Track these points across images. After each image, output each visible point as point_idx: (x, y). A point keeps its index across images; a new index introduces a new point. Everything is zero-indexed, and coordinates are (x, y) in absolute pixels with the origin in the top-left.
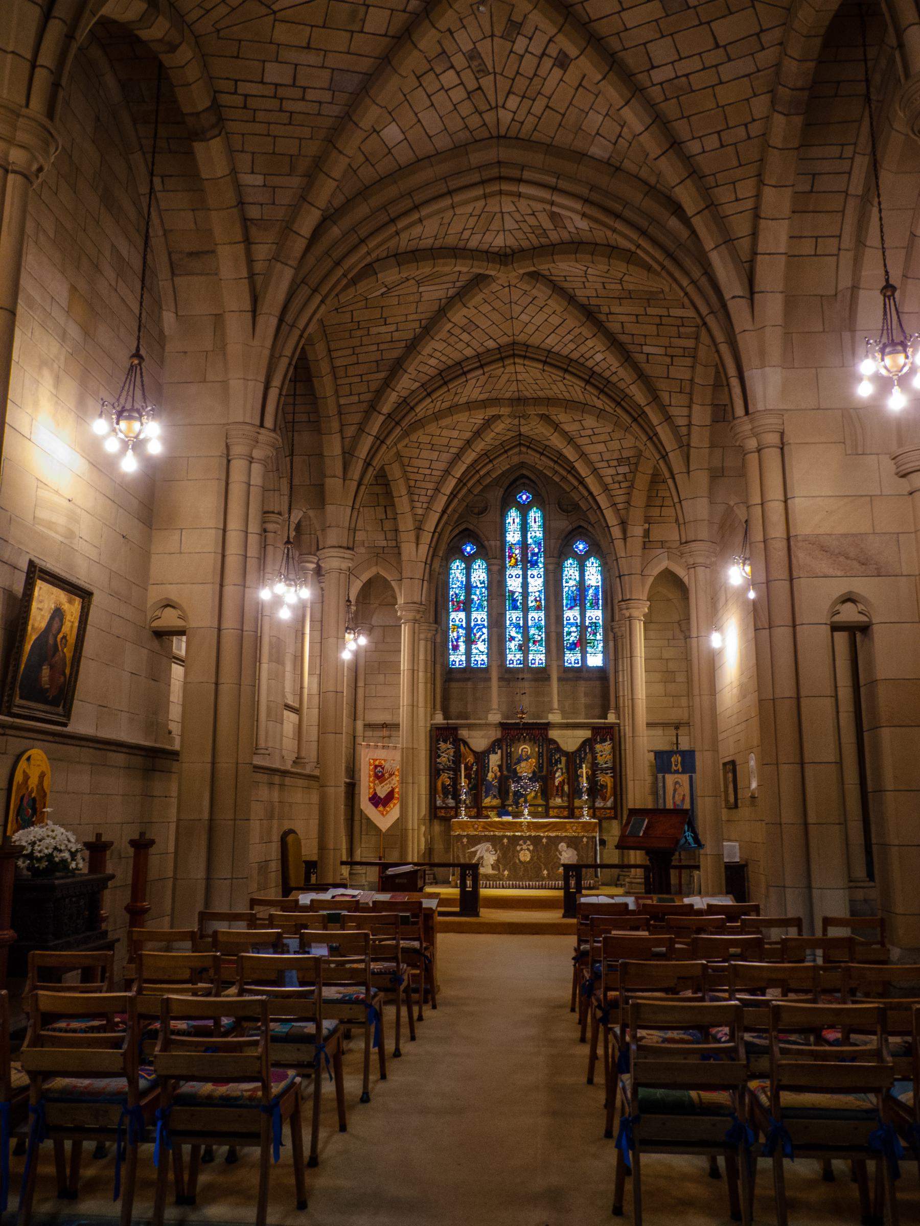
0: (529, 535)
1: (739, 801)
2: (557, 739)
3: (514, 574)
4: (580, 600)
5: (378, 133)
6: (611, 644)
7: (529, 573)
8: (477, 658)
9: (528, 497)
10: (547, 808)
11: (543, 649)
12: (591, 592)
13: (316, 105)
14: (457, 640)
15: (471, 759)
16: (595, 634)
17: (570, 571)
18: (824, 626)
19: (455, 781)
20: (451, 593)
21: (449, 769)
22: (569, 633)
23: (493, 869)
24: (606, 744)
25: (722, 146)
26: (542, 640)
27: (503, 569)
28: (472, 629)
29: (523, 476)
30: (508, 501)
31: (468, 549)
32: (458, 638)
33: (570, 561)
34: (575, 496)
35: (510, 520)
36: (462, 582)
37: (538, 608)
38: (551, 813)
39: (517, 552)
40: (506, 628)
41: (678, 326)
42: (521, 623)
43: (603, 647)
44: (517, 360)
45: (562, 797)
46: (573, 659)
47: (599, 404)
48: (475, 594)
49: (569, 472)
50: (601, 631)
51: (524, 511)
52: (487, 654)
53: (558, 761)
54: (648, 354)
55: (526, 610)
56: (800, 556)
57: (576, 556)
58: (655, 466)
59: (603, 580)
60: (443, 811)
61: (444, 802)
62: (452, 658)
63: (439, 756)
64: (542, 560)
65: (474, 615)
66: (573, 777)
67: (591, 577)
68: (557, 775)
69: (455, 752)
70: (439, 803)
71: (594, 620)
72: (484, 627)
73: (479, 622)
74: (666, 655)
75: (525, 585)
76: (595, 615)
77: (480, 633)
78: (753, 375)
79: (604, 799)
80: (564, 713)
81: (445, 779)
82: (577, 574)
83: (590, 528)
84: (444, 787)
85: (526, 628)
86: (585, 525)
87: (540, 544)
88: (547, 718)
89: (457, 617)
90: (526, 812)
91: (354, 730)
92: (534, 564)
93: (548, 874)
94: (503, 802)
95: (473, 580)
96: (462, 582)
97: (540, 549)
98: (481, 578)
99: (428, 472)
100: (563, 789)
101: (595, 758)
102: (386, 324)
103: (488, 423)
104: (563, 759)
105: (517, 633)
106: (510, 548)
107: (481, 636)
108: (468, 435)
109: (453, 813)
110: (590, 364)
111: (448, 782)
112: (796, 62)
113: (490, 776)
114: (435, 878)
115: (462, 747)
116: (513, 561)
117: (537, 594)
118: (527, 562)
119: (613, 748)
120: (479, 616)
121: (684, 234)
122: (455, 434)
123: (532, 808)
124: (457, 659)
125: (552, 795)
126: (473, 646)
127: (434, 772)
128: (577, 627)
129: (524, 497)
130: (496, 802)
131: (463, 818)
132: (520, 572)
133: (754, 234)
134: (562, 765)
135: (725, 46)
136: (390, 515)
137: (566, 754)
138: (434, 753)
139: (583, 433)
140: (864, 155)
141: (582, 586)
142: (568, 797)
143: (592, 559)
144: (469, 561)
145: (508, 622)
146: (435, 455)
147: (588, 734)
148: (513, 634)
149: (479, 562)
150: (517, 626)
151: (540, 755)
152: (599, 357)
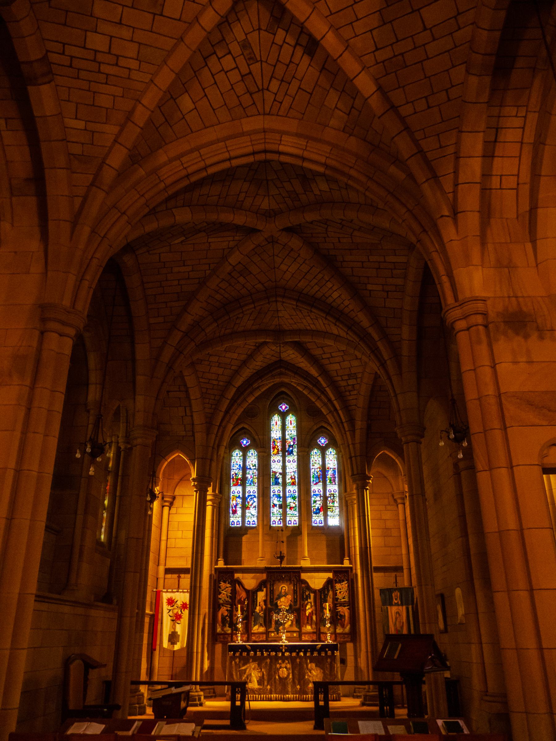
0: (287, 433)
1: (449, 627)
2: (308, 581)
3: (276, 460)
5: (175, 100)
6: (344, 508)
7: (287, 459)
8: (249, 520)
9: (286, 407)
10: (300, 633)
11: (296, 513)
12: (330, 473)
13: (127, 71)
14: (236, 507)
15: (243, 595)
16: (333, 502)
17: (315, 458)
18: (536, 467)
19: (231, 613)
20: (232, 473)
21: (227, 603)
22: (315, 502)
23: (258, 685)
24: (344, 583)
25: (429, 107)
26: (296, 505)
27: (269, 455)
28: (247, 499)
29: (283, 393)
30: (274, 409)
31: (245, 442)
32: (237, 505)
33: (315, 450)
34: (318, 404)
35: (273, 423)
36: (240, 465)
37: (293, 484)
38: (303, 638)
39: (279, 444)
40: (270, 498)
41: (392, 269)
42: (281, 494)
43: (340, 511)
44: (279, 299)
45: (311, 625)
46: (318, 521)
47: (335, 332)
48: (249, 474)
49: (314, 385)
50: (337, 499)
51: (284, 416)
52: (257, 517)
53: (308, 597)
54: (370, 290)
55: (284, 485)
56: (511, 409)
58: (377, 377)
59: (338, 464)
60: (222, 637)
61: (222, 629)
62: (232, 519)
63: (220, 593)
65: (248, 488)
66: (320, 610)
67: (330, 462)
68: (307, 608)
69: (232, 590)
70: (219, 630)
71: (332, 493)
72: (255, 497)
73: (251, 494)
74: (384, 517)
75: (284, 467)
76: (333, 488)
77: (252, 502)
78: (460, 273)
79: (343, 626)
80: (313, 561)
81: (223, 611)
82: (320, 460)
83: (329, 428)
84: (224, 618)
85: (285, 498)
86: (326, 426)
87: (295, 438)
88: (300, 564)
89: (236, 490)
90: (284, 637)
91: (157, 573)
92: (291, 453)
93: (300, 689)
94: (266, 630)
95: (247, 465)
96: (240, 465)
97: (294, 443)
98: (254, 463)
99: (215, 383)
100: (312, 619)
101: (336, 594)
102: (184, 266)
103: (259, 347)
104: (312, 595)
106: (274, 442)
108: (243, 357)
109: (229, 639)
110: (330, 300)
111: (226, 613)
112: (486, 32)
113: (258, 609)
114: (214, 692)
115: (237, 585)
116: (276, 451)
117: (293, 474)
118: (285, 452)
119: (348, 586)
120: (252, 489)
121: (402, 176)
122: (235, 356)
123: (289, 634)
124: (235, 520)
125: (304, 624)
126: (247, 511)
127: (215, 605)
128: (320, 497)
129: (284, 407)
130: (262, 629)
132: (281, 459)
133: (456, 172)
134: (311, 600)
135: (430, 29)
136: (188, 413)
137: (314, 591)
138: (215, 591)
139: (324, 356)
140: (535, 112)
141: (324, 469)
142: (316, 624)
143: (330, 450)
144: (245, 450)
145: (272, 494)
146: (220, 371)
147: (330, 575)
148: (276, 502)
149: (252, 451)
150: (278, 497)
151: (295, 592)
152: (335, 295)
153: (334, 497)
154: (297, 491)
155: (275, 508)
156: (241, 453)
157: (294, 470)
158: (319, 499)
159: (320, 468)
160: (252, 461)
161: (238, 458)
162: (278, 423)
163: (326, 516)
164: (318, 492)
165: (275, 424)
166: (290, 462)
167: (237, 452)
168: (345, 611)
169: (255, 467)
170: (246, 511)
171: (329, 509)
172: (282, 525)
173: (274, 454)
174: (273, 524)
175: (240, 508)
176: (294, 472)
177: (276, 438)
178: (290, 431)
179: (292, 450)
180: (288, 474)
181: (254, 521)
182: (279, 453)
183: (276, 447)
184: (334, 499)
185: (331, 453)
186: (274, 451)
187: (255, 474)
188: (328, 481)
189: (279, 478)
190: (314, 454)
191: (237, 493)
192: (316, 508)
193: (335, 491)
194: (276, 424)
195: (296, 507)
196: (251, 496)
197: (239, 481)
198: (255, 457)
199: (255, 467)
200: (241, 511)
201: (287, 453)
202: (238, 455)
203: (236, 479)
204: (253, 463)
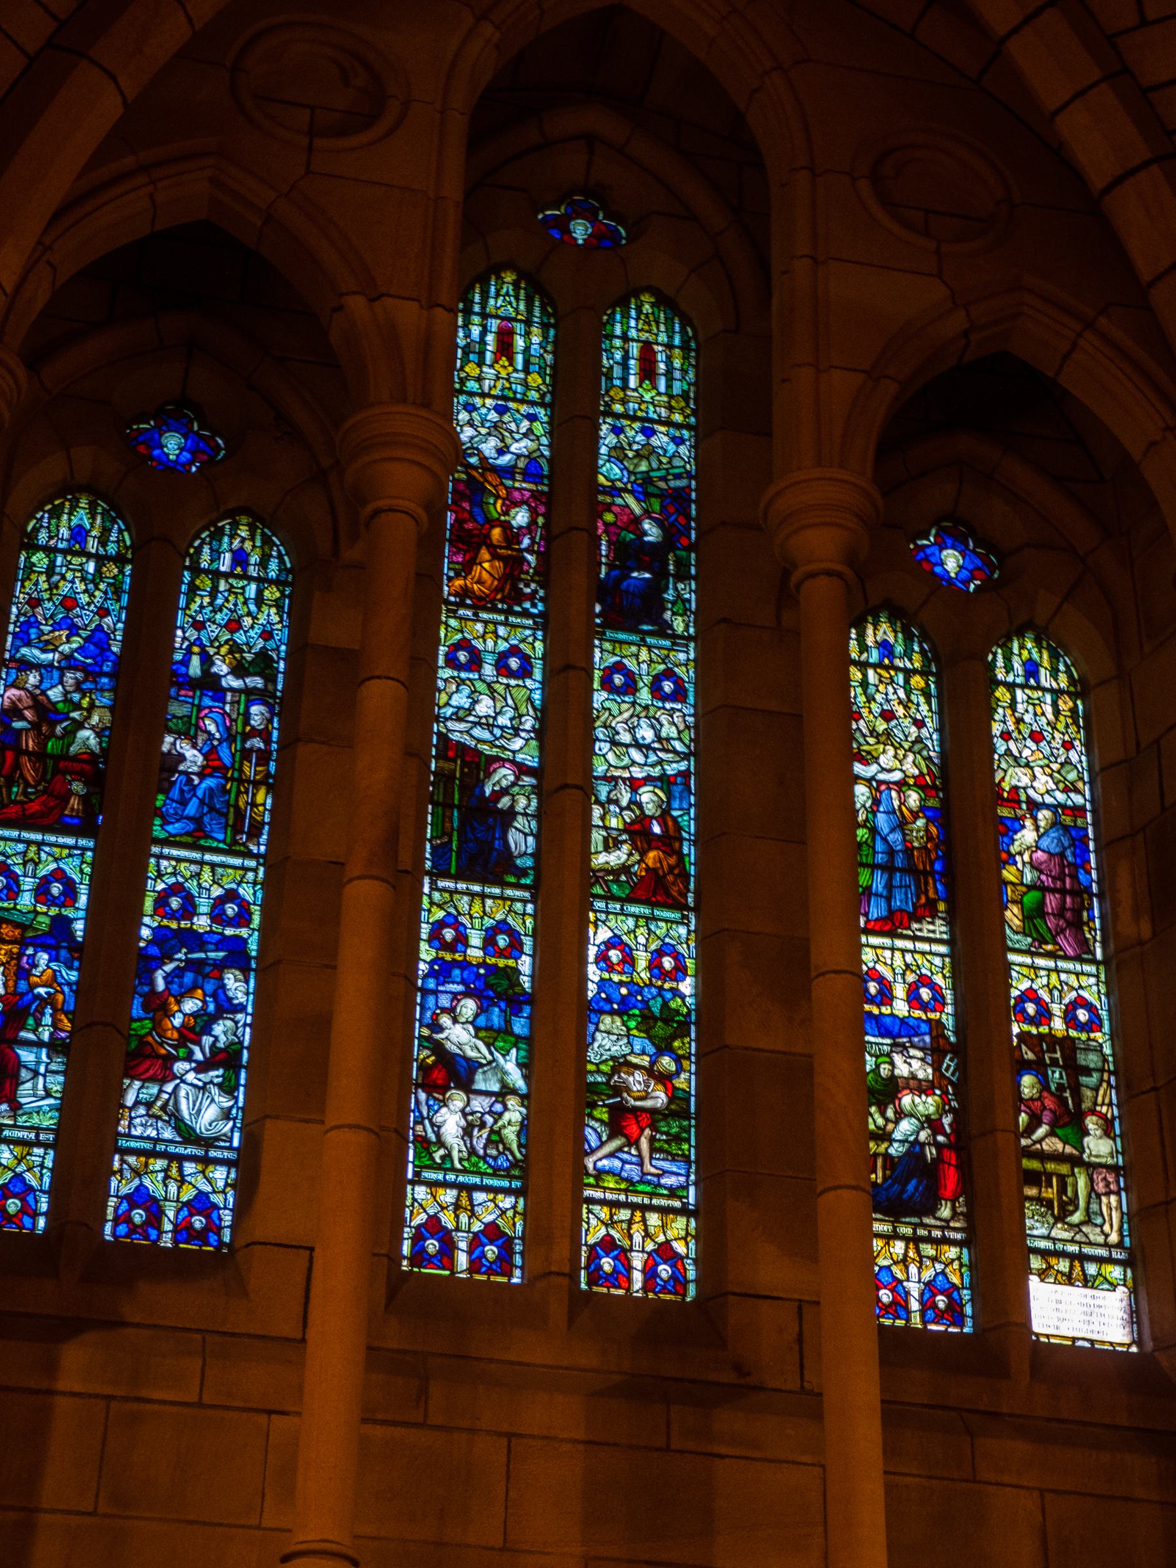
4: (949, 875)
7: (601, 658)
8: (155, 1185)
26: (674, 1095)
28: (148, 964)
33: (882, 631)
36: (99, 639)
39: (520, 517)
46: (914, 1288)
48: (191, 730)
64: (688, 591)
72: (236, 954)
73: (202, 923)
96: (99, 639)
98: (250, 637)
105: (489, 1034)
107: (201, 1024)
116: (487, 568)
128: (936, 1052)
129: (580, 231)
143: (1026, 649)
145: (426, 953)
153: (1075, 1070)
154: (690, 964)
155: (458, 1099)
156: (119, 538)
157: (671, 770)
158: (924, 1072)
159: (919, 784)
160: (234, 625)
161: (91, 567)
162: (520, 343)
164: (913, 998)
165: (490, 338)
166: (630, 687)
167: (81, 517)
169: (257, 682)
170: (122, 1093)
171: (1033, 1178)
172: (515, 1280)
173: (465, 592)
174: (419, 1256)
175: (53, 1046)
176: (665, 781)
177: (506, 459)
178: (633, 432)
179: (655, 589)
180: (603, 791)
181: (201, 1204)
182: (519, 597)
183: (496, 533)
184: (1076, 1089)
185: (1031, 669)
186: (466, 569)
187: (258, 743)
188: (1013, 915)
189: (511, 814)
190: (874, 657)
191: (42, 892)
192: (896, 1150)
193: (1082, 1015)
194: (505, 348)
195: (677, 1108)
196: (194, 940)
197: (77, 787)
198: (271, 593)
199: (257, 682)
200: (56, 1083)
201: (598, 608)
202: (92, 545)
203: (40, 756)
204: (240, 637)
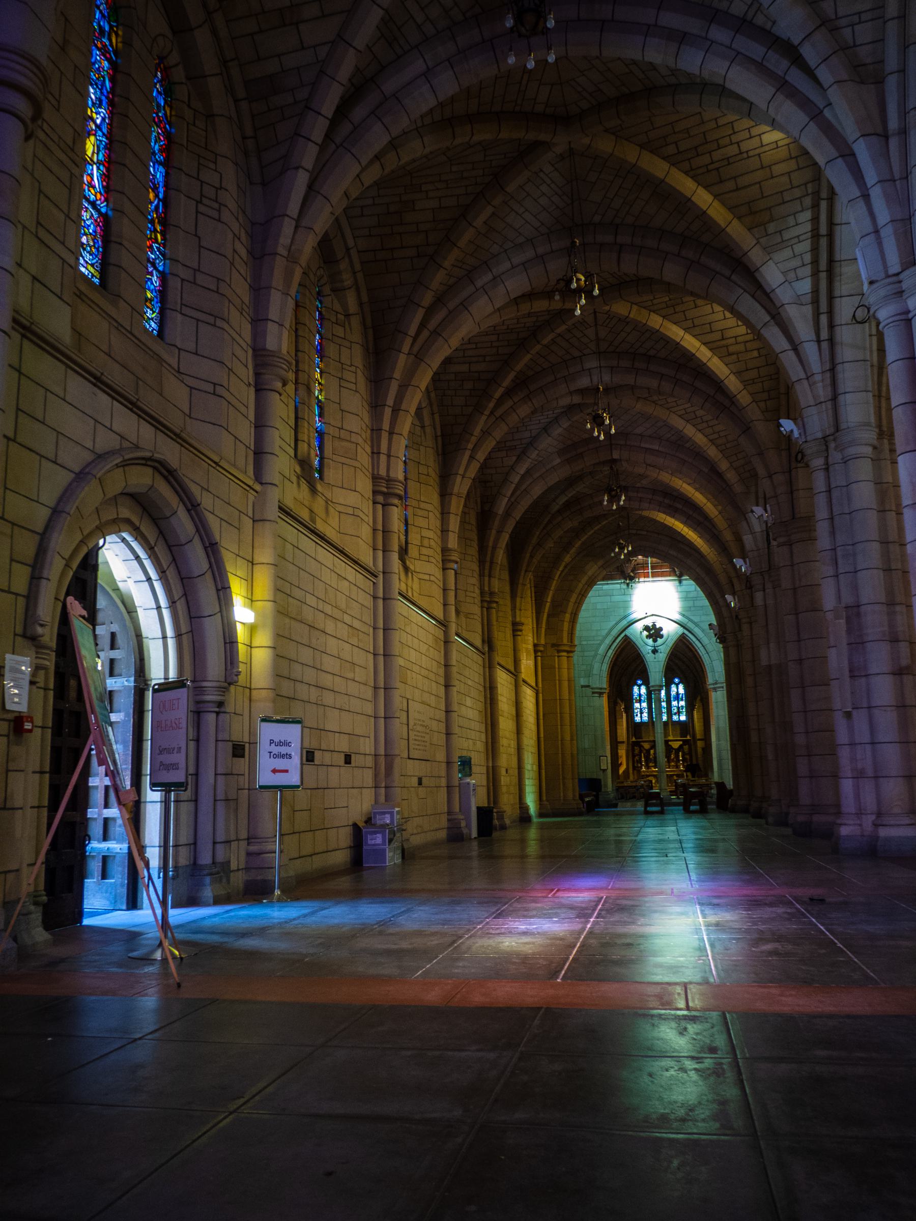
17: (674, 689)
33: (673, 686)
57: (675, 683)
65: (643, 704)
66: (677, 756)
76: (682, 703)
80: (674, 737)
81: (637, 758)
89: (637, 705)
120: (645, 705)
124: (638, 719)
131: (644, 769)
138: (633, 750)
141: (678, 694)
144: (639, 686)
147: (681, 743)
163: (679, 716)
168: (688, 757)
